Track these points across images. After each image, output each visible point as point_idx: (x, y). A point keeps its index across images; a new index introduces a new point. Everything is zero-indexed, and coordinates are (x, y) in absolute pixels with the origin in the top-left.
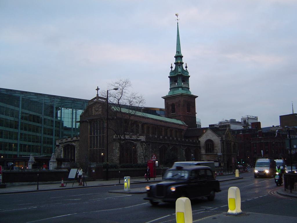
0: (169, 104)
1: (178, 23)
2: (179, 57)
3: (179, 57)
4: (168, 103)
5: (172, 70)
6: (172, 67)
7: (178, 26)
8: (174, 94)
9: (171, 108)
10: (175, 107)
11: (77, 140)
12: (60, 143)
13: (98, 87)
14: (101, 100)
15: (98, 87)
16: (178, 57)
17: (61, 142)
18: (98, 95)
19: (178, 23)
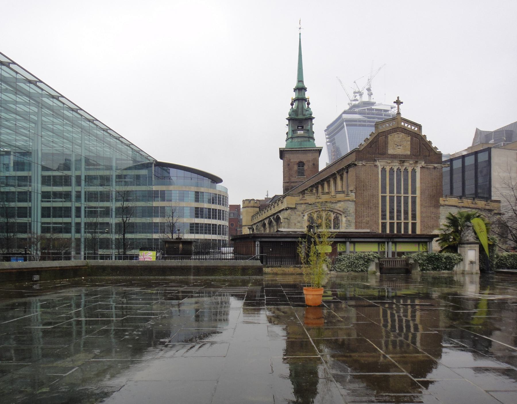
0: (292, 161)
1: (300, 34)
2: (300, 89)
3: (300, 89)
4: (290, 160)
5: (292, 108)
6: (292, 104)
7: (300, 39)
8: (303, 147)
9: (296, 167)
10: (306, 167)
11: (349, 200)
12: (297, 204)
13: (398, 98)
14: (406, 125)
15: (398, 98)
16: (303, 90)
17: (302, 202)
18: (399, 113)
19: (300, 34)
